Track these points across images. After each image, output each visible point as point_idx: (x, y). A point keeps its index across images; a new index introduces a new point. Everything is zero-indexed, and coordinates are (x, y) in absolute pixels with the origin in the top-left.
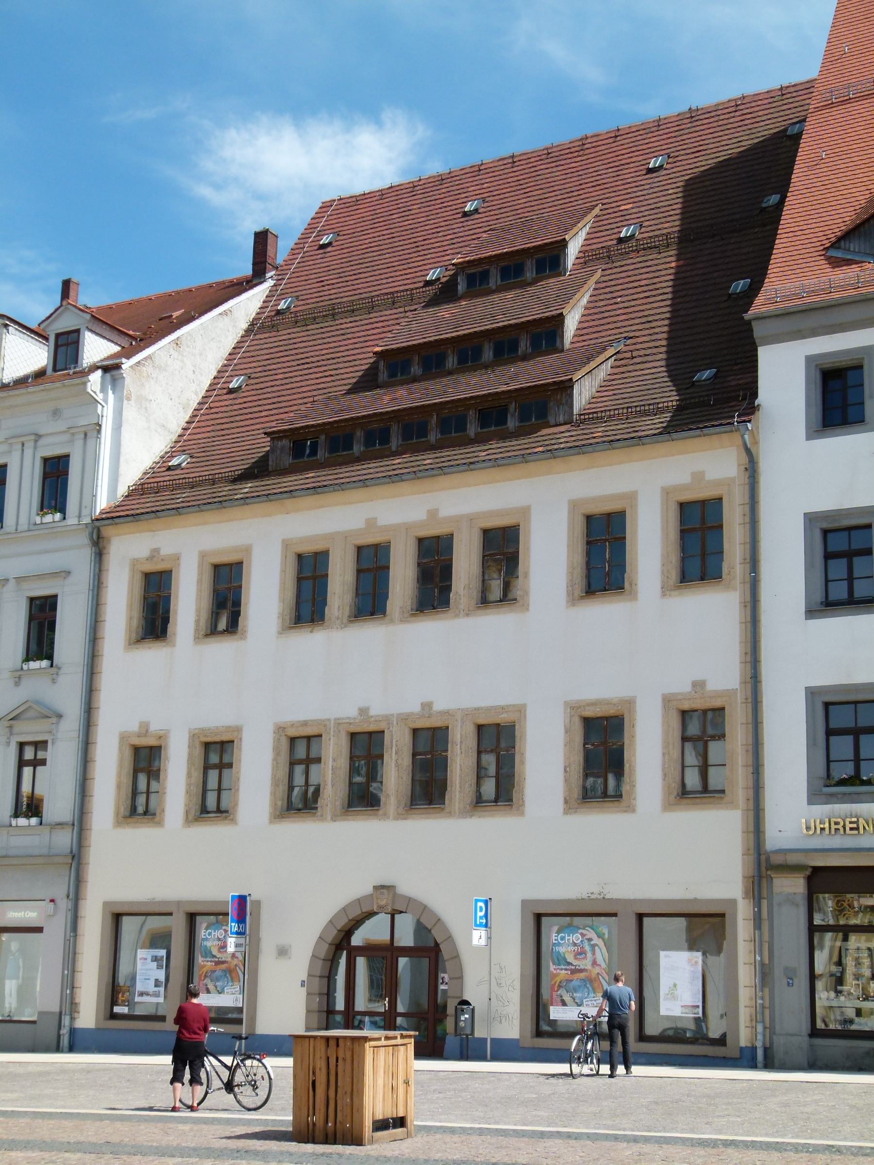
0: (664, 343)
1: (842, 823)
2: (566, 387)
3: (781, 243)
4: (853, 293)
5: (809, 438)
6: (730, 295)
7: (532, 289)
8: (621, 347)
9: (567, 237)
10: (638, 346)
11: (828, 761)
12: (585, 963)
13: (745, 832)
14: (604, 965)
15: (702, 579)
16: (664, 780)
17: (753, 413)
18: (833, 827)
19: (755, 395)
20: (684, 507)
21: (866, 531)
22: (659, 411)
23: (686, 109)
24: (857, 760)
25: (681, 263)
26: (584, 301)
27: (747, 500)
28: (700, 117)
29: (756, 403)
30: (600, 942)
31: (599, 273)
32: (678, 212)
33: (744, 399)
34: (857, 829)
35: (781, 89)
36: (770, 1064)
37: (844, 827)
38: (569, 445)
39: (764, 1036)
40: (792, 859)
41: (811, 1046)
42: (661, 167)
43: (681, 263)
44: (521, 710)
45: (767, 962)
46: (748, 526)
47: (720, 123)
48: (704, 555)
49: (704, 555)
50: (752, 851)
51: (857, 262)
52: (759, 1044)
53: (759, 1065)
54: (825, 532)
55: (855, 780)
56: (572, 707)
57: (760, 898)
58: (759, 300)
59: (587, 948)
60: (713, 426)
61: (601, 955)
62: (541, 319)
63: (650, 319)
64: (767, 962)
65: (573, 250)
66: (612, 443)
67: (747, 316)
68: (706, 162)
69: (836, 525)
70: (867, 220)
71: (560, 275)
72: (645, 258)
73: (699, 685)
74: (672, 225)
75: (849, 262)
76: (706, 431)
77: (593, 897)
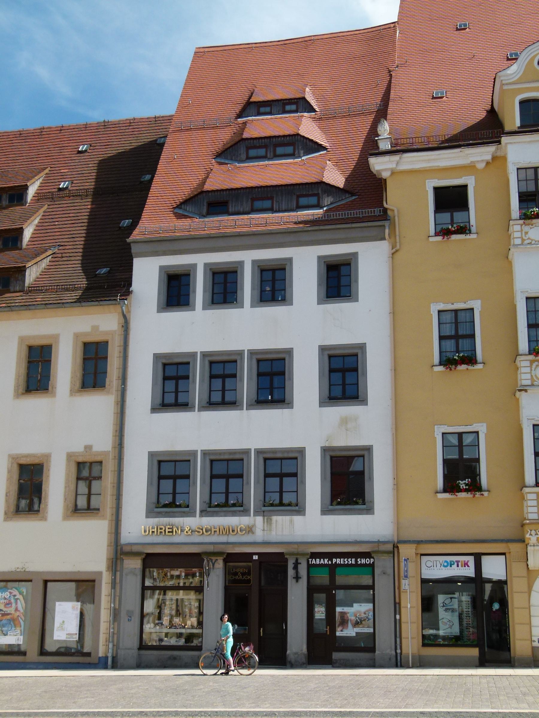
0: (81, 250)
1: (164, 529)
2: (21, 271)
3: (150, 201)
4: (187, 234)
5: (159, 311)
6: (120, 227)
7: (5, 212)
8: (56, 250)
9: (28, 184)
10: (66, 251)
11: (159, 494)
12: (11, 610)
13: (110, 533)
14: (22, 611)
15: (94, 387)
16: (65, 502)
17: (128, 295)
18: (159, 531)
19: (130, 285)
20: (86, 345)
21: (186, 366)
22: (75, 289)
23: (102, 120)
24: (174, 493)
25: (94, 206)
26: (36, 222)
27: (122, 343)
28: (110, 126)
29: (131, 289)
30: (21, 597)
31: (46, 207)
32: (94, 177)
33: (124, 286)
34: (172, 532)
35: (155, 117)
36: (115, 666)
37: (165, 531)
38: (21, 304)
39: (113, 650)
40: (135, 549)
41: (139, 655)
42: (86, 151)
43: (94, 206)
45: (117, 607)
46: (121, 359)
47: (121, 131)
48: (95, 374)
49: (95, 374)
50: (113, 544)
51: (190, 217)
52: (110, 655)
53: (109, 667)
54: (165, 365)
55: (172, 504)
56: (13, 458)
57: (116, 571)
58: (136, 232)
59: (13, 601)
60: (106, 300)
61: (21, 605)
62: (9, 229)
63: (74, 236)
64: (117, 607)
65: (32, 191)
66: (46, 305)
67: (128, 240)
68: (112, 152)
69: (170, 361)
70: (197, 195)
71: (23, 205)
72: (73, 201)
73: (88, 448)
74: (90, 184)
75: (186, 217)
76: (101, 303)
77: (18, 570)
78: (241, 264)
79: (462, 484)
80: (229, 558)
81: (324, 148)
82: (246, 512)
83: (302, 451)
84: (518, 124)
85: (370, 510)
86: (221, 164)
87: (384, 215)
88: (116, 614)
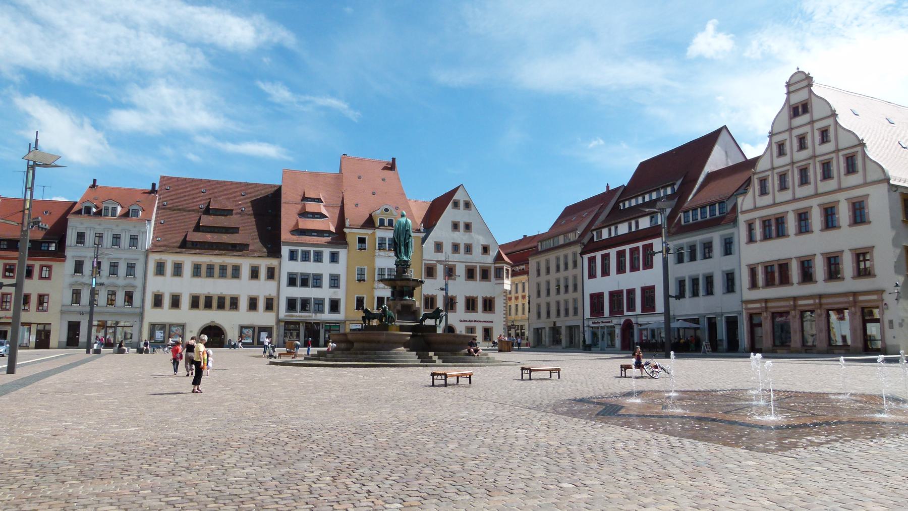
40: (283, 320)
44: (239, 295)
78: (310, 251)
79: (361, 308)
80: (306, 323)
81: (328, 217)
82: (311, 313)
83: (324, 299)
84: (379, 224)
85: (339, 313)
86: (300, 218)
87: (346, 243)
88: (278, 336)
